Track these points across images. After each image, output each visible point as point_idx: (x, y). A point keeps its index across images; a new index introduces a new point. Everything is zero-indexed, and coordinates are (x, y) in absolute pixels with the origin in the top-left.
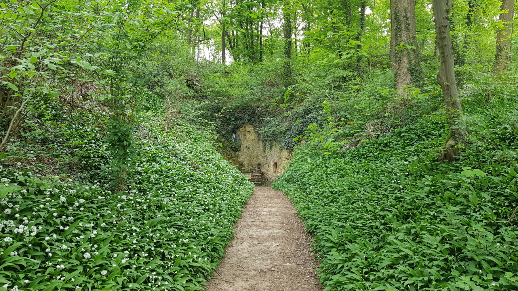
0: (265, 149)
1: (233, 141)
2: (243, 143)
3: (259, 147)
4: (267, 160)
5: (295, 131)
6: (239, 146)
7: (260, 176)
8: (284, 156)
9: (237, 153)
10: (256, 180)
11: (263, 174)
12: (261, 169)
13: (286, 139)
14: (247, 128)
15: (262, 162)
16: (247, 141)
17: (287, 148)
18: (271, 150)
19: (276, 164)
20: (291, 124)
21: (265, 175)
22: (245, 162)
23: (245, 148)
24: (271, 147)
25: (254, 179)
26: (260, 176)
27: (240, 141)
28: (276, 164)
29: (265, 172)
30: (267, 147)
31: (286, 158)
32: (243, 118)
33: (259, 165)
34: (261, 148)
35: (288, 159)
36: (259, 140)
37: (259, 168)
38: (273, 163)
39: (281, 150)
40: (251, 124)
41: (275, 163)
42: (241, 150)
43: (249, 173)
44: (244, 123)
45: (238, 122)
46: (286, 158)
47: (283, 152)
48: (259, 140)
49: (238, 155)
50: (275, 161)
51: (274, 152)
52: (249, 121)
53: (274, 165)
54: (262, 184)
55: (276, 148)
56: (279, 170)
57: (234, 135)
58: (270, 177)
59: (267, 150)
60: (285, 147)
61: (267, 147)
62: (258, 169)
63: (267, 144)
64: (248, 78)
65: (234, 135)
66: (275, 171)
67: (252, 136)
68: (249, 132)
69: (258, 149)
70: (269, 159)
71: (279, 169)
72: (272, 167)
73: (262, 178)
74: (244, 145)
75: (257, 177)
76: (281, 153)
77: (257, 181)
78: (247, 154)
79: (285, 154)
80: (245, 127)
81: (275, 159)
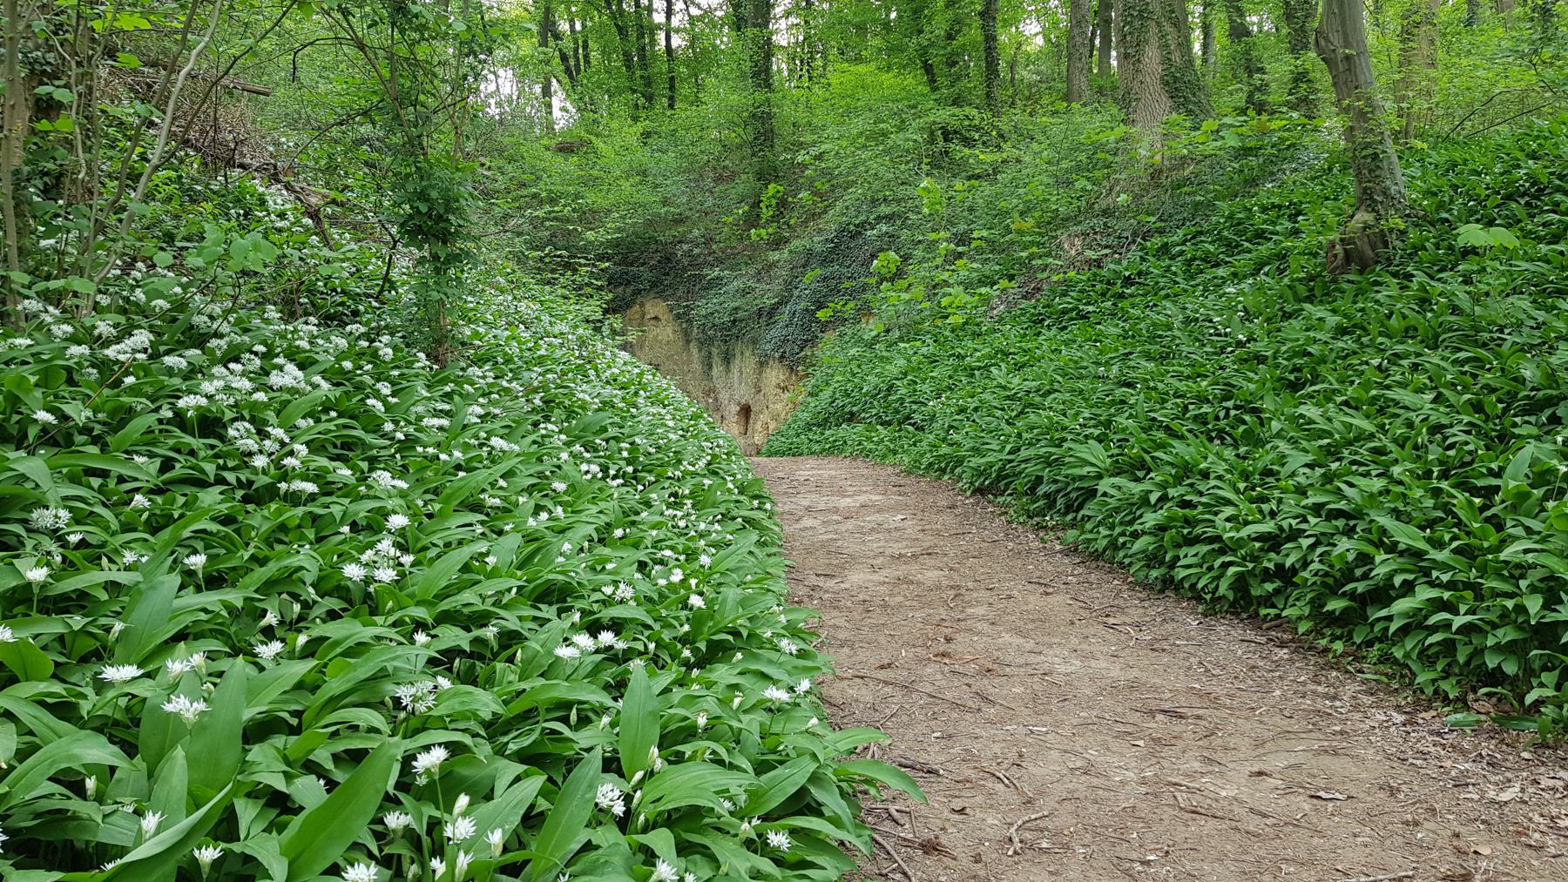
0: (710, 368)
3: (689, 362)
4: (716, 399)
5: (803, 305)
8: (774, 381)
13: (776, 332)
14: (648, 307)
17: (782, 357)
18: (728, 370)
19: (746, 411)
20: (790, 285)
24: (727, 359)
28: (746, 411)
30: (716, 360)
31: (778, 386)
32: (636, 278)
34: (697, 366)
35: (785, 389)
36: (688, 342)
38: (735, 409)
39: (762, 364)
40: (661, 295)
44: (638, 292)
45: (620, 290)
46: (778, 386)
47: (768, 370)
50: (743, 402)
51: (737, 374)
52: (654, 285)
55: (745, 363)
56: (758, 426)
59: (717, 370)
60: (777, 355)
61: (716, 360)
63: (715, 351)
64: (642, 156)
66: (742, 430)
68: (656, 318)
70: (724, 396)
71: (760, 423)
72: (735, 420)
76: (760, 373)
79: (775, 375)
80: (642, 305)
81: (743, 393)
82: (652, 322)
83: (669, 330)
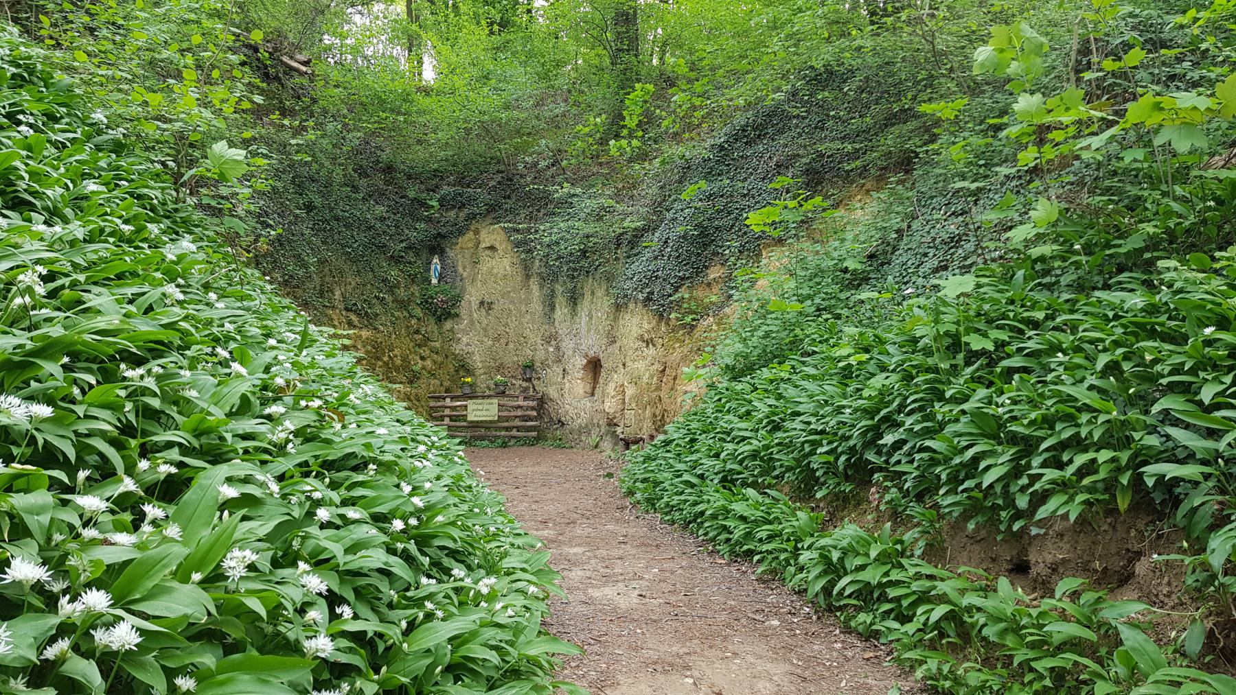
0: (553, 309)
1: (434, 281)
2: (469, 288)
3: (528, 301)
4: (558, 348)
5: (680, 230)
6: (456, 300)
7: (533, 408)
8: (635, 332)
9: (448, 325)
10: (518, 423)
11: (542, 401)
12: (535, 382)
13: (638, 266)
15: (540, 355)
16: (484, 283)
17: (648, 299)
18: (574, 313)
19: (594, 366)
20: (660, 207)
21: (550, 407)
22: (477, 357)
23: (475, 305)
24: (574, 299)
25: (507, 419)
26: (533, 408)
27: (458, 283)
28: (594, 366)
29: (552, 392)
30: (560, 300)
31: (641, 338)
32: (471, 200)
33: (529, 367)
34: (537, 306)
35: (649, 342)
36: (528, 277)
37: (529, 380)
38: (581, 362)
39: (618, 308)
41: (589, 362)
42: (463, 312)
43: (489, 397)
44: (472, 217)
45: (452, 214)
46: (641, 338)
47: (627, 316)
48: (528, 277)
49: (452, 330)
50: (591, 354)
51: (585, 319)
53: (585, 368)
54: (538, 439)
55: (597, 304)
56: (611, 389)
57: (436, 260)
58: (572, 412)
59: (561, 312)
60: (640, 296)
61: (560, 300)
62: (525, 384)
63: (559, 289)
65: (436, 260)
66: (588, 388)
67: (503, 264)
68: (492, 248)
69: (523, 308)
70: (568, 345)
71: (612, 386)
72: (580, 375)
73: (539, 417)
74: (472, 296)
75: (519, 413)
76: (616, 319)
77: (518, 429)
78: (485, 330)
79: (636, 323)
80: (477, 232)
81: (592, 343)
82: (488, 252)
83: (506, 262)
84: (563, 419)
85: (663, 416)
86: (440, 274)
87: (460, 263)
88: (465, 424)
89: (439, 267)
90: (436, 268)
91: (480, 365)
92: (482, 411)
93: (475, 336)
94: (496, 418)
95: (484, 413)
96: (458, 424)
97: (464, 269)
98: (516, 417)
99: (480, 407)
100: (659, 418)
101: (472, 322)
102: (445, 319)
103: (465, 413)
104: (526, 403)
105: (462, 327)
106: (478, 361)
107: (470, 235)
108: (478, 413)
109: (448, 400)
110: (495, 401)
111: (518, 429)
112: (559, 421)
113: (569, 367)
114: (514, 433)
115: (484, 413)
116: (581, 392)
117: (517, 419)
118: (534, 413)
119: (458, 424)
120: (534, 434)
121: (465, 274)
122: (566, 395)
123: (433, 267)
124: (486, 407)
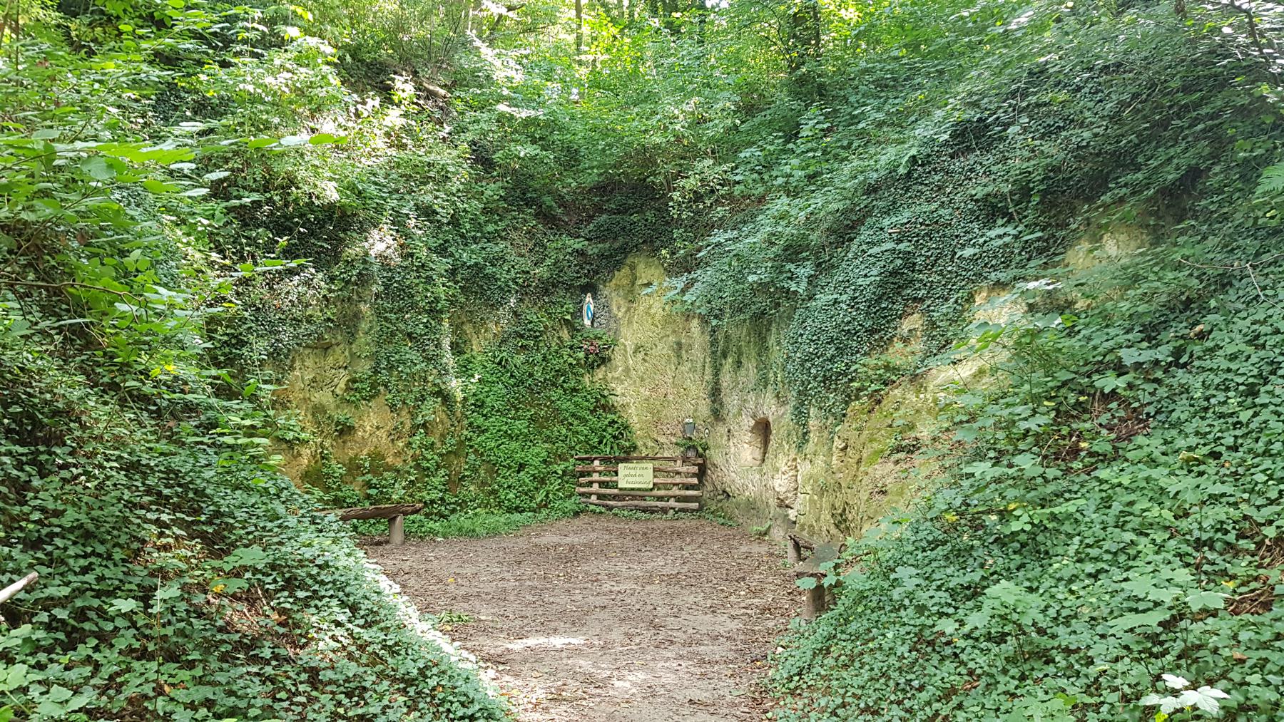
2: (624, 330)
6: (611, 345)
7: (694, 475)
10: (675, 491)
22: (632, 410)
25: (666, 487)
26: (694, 475)
27: (612, 325)
41: (757, 423)
42: (617, 358)
43: (646, 458)
57: (589, 298)
65: (589, 298)
66: (758, 454)
74: (628, 338)
75: (678, 480)
77: (678, 499)
78: (642, 380)
80: (633, 267)
84: (728, 489)
85: (844, 510)
86: (594, 315)
87: (614, 303)
88: (616, 491)
89: (592, 307)
90: (589, 308)
91: (636, 419)
92: (633, 476)
93: (630, 385)
94: (651, 486)
95: (638, 479)
96: (608, 491)
97: (619, 308)
98: (674, 485)
99: (633, 472)
100: (840, 511)
101: (627, 370)
102: (599, 366)
103: (615, 478)
104: (684, 469)
105: (616, 375)
106: (635, 417)
107: (626, 271)
108: (630, 479)
109: (597, 463)
110: (650, 465)
111: (678, 499)
112: (724, 491)
113: (734, 427)
114: (672, 503)
115: (638, 479)
116: (749, 458)
117: (675, 488)
118: (695, 481)
119: (608, 491)
120: (695, 505)
121: (620, 315)
122: (731, 461)
123: (585, 308)
124: (639, 472)
